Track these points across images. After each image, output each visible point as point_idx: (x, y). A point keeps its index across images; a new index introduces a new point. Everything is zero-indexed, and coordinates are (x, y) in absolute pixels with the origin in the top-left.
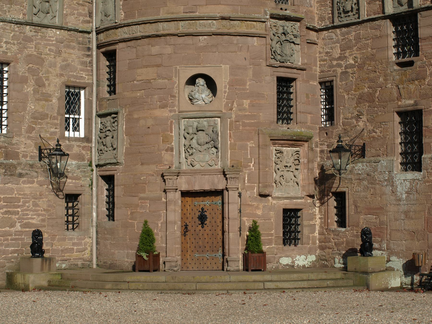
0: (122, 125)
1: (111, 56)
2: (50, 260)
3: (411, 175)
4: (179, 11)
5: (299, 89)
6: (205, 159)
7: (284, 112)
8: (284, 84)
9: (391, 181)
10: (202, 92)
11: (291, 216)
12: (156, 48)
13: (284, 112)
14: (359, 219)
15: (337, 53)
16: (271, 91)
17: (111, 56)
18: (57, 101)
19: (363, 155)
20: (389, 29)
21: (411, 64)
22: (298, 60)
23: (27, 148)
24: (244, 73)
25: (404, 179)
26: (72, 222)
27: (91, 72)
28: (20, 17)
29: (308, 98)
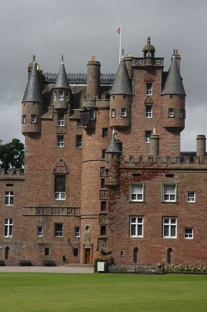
16: (99, 229)
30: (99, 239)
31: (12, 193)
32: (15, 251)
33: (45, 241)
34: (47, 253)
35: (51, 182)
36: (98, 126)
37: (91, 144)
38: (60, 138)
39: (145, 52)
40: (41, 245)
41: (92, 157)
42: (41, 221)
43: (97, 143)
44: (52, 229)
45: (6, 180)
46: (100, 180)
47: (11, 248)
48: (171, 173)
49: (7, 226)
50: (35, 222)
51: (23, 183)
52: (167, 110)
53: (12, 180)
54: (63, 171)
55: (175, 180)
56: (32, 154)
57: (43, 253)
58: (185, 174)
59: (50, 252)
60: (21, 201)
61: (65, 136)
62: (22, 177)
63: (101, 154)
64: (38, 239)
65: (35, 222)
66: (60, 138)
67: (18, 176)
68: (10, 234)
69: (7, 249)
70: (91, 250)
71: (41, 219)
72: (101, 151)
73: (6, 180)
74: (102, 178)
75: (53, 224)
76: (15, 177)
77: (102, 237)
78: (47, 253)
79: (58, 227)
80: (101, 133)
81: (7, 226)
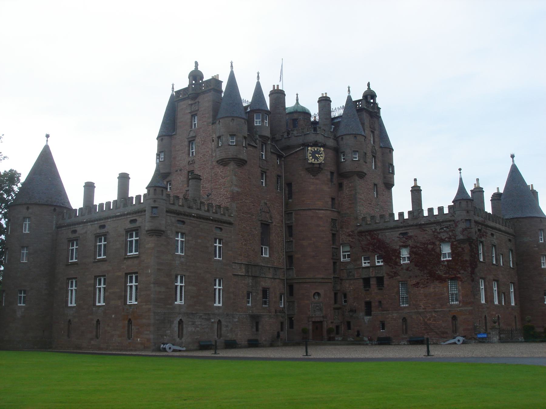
0: (296, 304)
2: (282, 339)
3: (368, 317)
5: (339, 295)
6: (318, 313)
7: (336, 302)
8: (336, 294)
9: (363, 319)
10: (317, 297)
15: (347, 286)
19: (355, 312)
20: (361, 281)
21: (368, 290)
22: (338, 288)
25: (367, 318)
26: (282, 330)
28: (271, 277)
30: (335, 309)
32: (227, 326)
36: (326, 168)
42: (251, 284)
44: (260, 296)
45: (215, 221)
46: (331, 235)
47: (224, 323)
49: (215, 289)
52: (387, 164)
53: (221, 222)
56: (239, 190)
57: (254, 329)
59: (260, 327)
62: (231, 220)
63: (330, 203)
66: (263, 173)
67: (226, 218)
68: (219, 303)
69: (219, 322)
70: (325, 323)
71: (250, 281)
72: (330, 200)
73: (215, 221)
74: (333, 232)
75: (261, 288)
77: (336, 306)
79: (265, 292)
80: (329, 177)
81: (215, 289)
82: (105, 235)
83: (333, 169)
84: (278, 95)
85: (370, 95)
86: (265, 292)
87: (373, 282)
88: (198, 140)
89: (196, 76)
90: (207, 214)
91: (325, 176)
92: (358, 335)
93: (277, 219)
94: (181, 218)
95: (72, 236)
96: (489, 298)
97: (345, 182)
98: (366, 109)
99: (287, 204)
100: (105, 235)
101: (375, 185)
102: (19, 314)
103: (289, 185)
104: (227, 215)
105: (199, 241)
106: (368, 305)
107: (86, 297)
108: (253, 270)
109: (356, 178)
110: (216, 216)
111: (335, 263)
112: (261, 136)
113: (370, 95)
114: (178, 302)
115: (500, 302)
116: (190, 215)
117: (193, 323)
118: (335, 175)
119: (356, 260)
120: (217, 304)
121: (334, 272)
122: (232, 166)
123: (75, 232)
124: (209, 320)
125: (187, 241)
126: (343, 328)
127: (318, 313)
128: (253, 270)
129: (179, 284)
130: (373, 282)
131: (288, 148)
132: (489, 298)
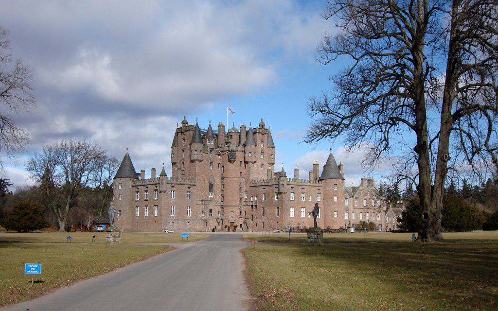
1: (223, 208)
4: (230, 204)
5: (242, 212)
6: (232, 219)
7: (240, 214)
8: (241, 212)
10: (232, 212)
11: (241, 225)
12: (227, 208)
13: (240, 214)
14: (248, 225)
17: (223, 208)
18: (217, 213)
23: (214, 218)
24: (236, 211)
25: (252, 221)
27: (221, 210)
29: (243, 213)
31: (190, 192)
33: (206, 218)
34: (206, 225)
35: (207, 187)
37: (234, 168)
38: (211, 163)
39: (260, 125)
40: (204, 220)
41: (234, 175)
43: (237, 168)
48: (303, 187)
50: (201, 208)
51: (195, 187)
54: (212, 181)
55: (304, 190)
58: (308, 187)
60: (194, 197)
61: (213, 163)
62: (195, 184)
63: (239, 175)
64: (202, 217)
65: (201, 208)
66: (211, 163)
67: (193, 183)
76: (192, 184)
78: (206, 225)
79: (211, 211)
82: (148, 191)
83: (242, 160)
84: (221, 126)
85: (262, 126)
86: (211, 211)
87: (254, 207)
88: (185, 150)
89: (184, 122)
90: (184, 183)
91: (237, 163)
92: (248, 228)
93: (218, 181)
94: (173, 185)
95: (137, 190)
96: (298, 214)
97: (247, 165)
98: (262, 130)
99: (222, 175)
100: (148, 191)
101: (262, 165)
102: (119, 219)
103: (223, 167)
104: (193, 182)
105: (181, 193)
106: (252, 215)
107: (142, 213)
108: (205, 202)
109: (251, 163)
110: (189, 183)
111: (241, 199)
112: (210, 148)
113: (262, 126)
114: (172, 215)
115: (306, 216)
116: (176, 184)
117: (178, 223)
118: (243, 163)
119: (249, 198)
120: (188, 216)
121: (240, 202)
122: (196, 162)
123: (138, 188)
124: (185, 221)
125: (176, 194)
126: (243, 226)
127: (232, 219)
128: (205, 202)
129: (172, 209)
130: (254, 207)
131: (222, 152)
132: (298, 214)
